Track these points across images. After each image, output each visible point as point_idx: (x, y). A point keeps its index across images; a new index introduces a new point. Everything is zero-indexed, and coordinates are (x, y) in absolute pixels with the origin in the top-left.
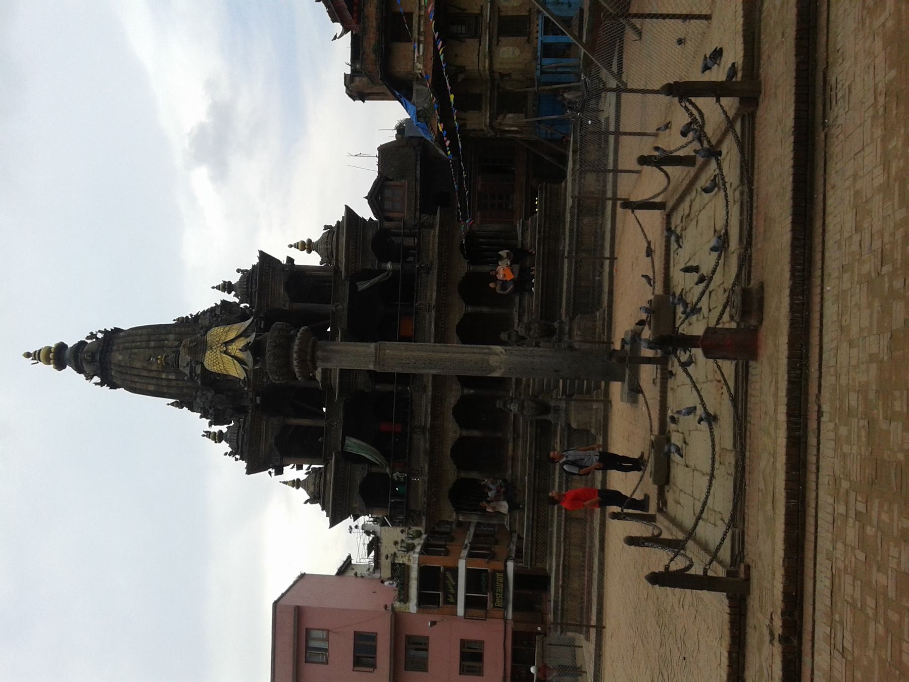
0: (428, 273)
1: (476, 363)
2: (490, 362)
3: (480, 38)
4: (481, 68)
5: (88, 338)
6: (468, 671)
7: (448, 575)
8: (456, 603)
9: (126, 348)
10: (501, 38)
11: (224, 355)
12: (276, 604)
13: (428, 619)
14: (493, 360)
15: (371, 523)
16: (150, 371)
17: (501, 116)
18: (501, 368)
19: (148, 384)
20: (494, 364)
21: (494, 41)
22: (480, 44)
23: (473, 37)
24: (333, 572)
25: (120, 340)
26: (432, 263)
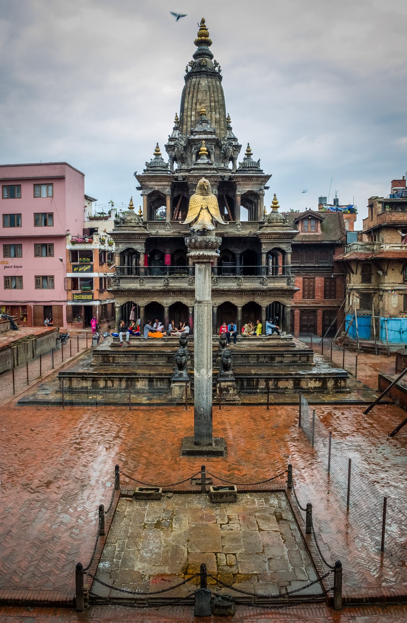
1: (202, 361)
3: (404, 284)
4: (385, 285)
5: (215, 61)
6: (37, 280)
7: (89, 267)
8: (73, 272)
9: (209, 88)
10: (403, 296)
12: (65, 164)
13: (64, 257)
14: (203, 371)
16: (196, 104)
17: (358, 295)
19: (188, 103)
20: (201, 372)
21: (401, 292)
22: (399, 284)
23: (404, 279)
24: (86, 193)
25: (214, 82)
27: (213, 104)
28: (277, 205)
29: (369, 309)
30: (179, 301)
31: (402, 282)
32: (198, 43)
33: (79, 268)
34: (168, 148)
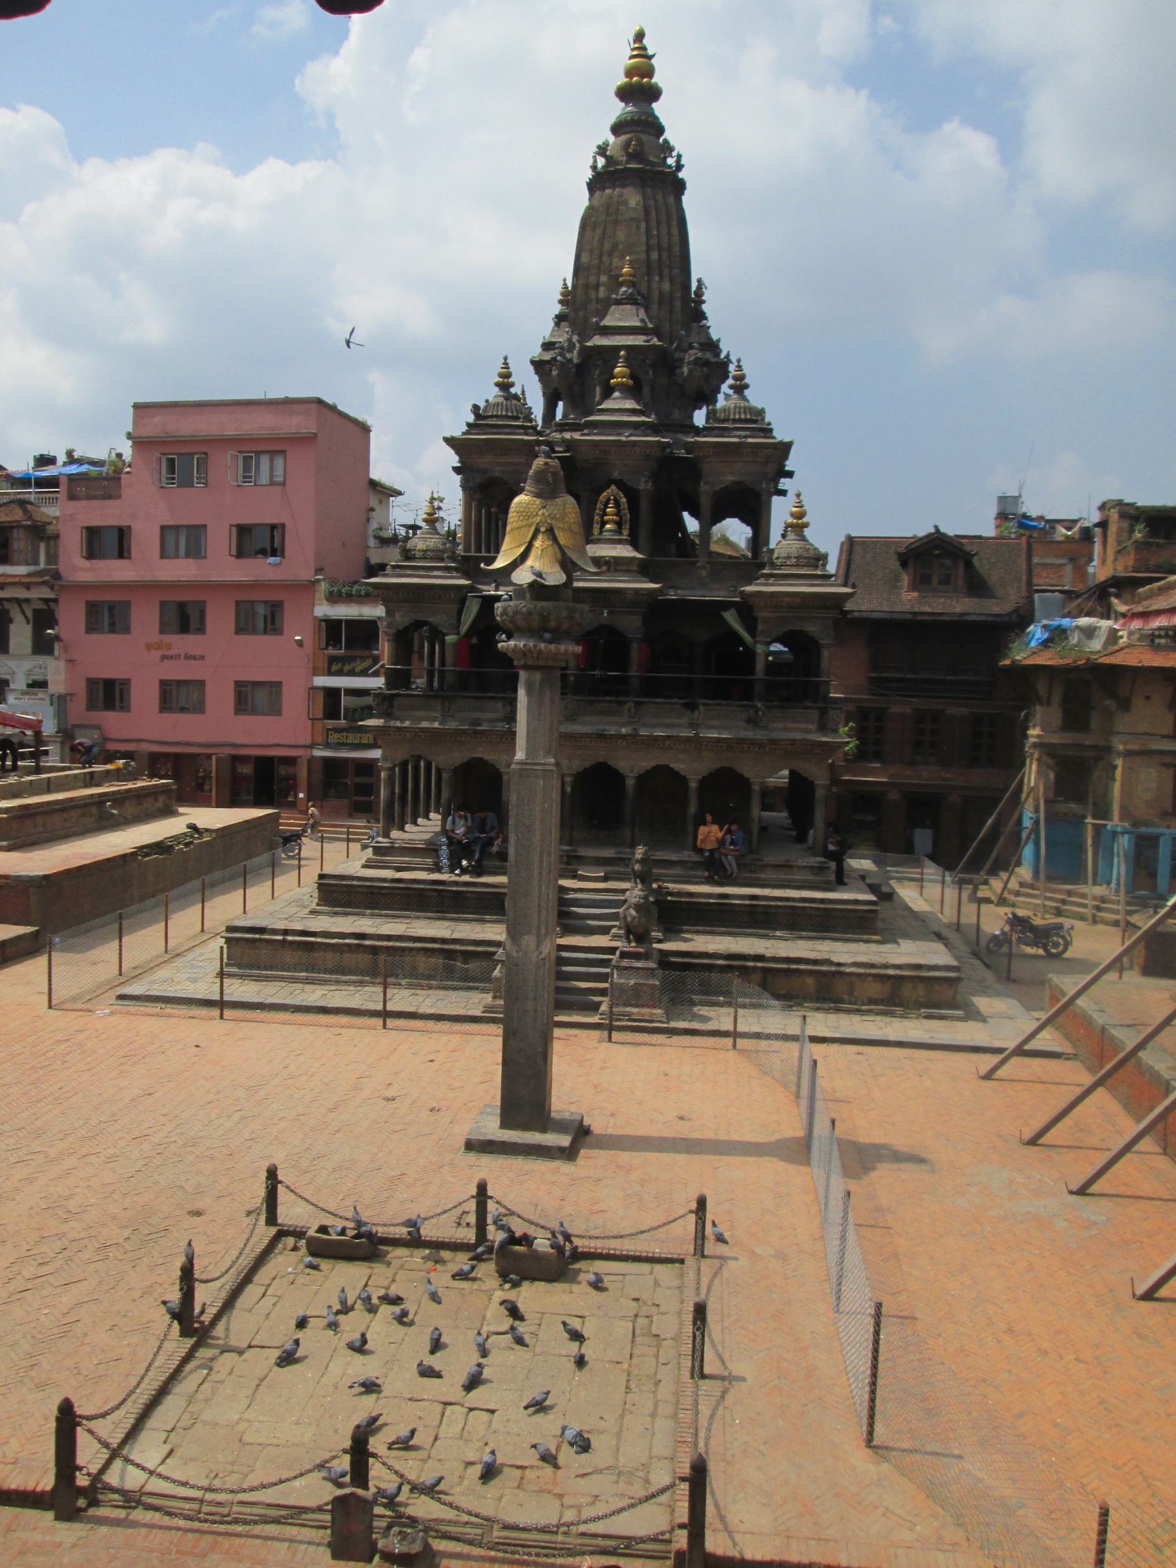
0: (749, 721)
8: (330, 673)
9: (647, 211)
11: (533, 529)
12: (319, 402)
15: (446, 529)
16: (610, 254)
18: (517, 951)
20: (524, 942)
21: (1168, 759)
24: (375, 475)
25: (660, 197)
26: (765, 728)
28: (805, 520)
31: (1171, 732)
32: (624, 94)
33: (344, 665)
34: (539, 366)
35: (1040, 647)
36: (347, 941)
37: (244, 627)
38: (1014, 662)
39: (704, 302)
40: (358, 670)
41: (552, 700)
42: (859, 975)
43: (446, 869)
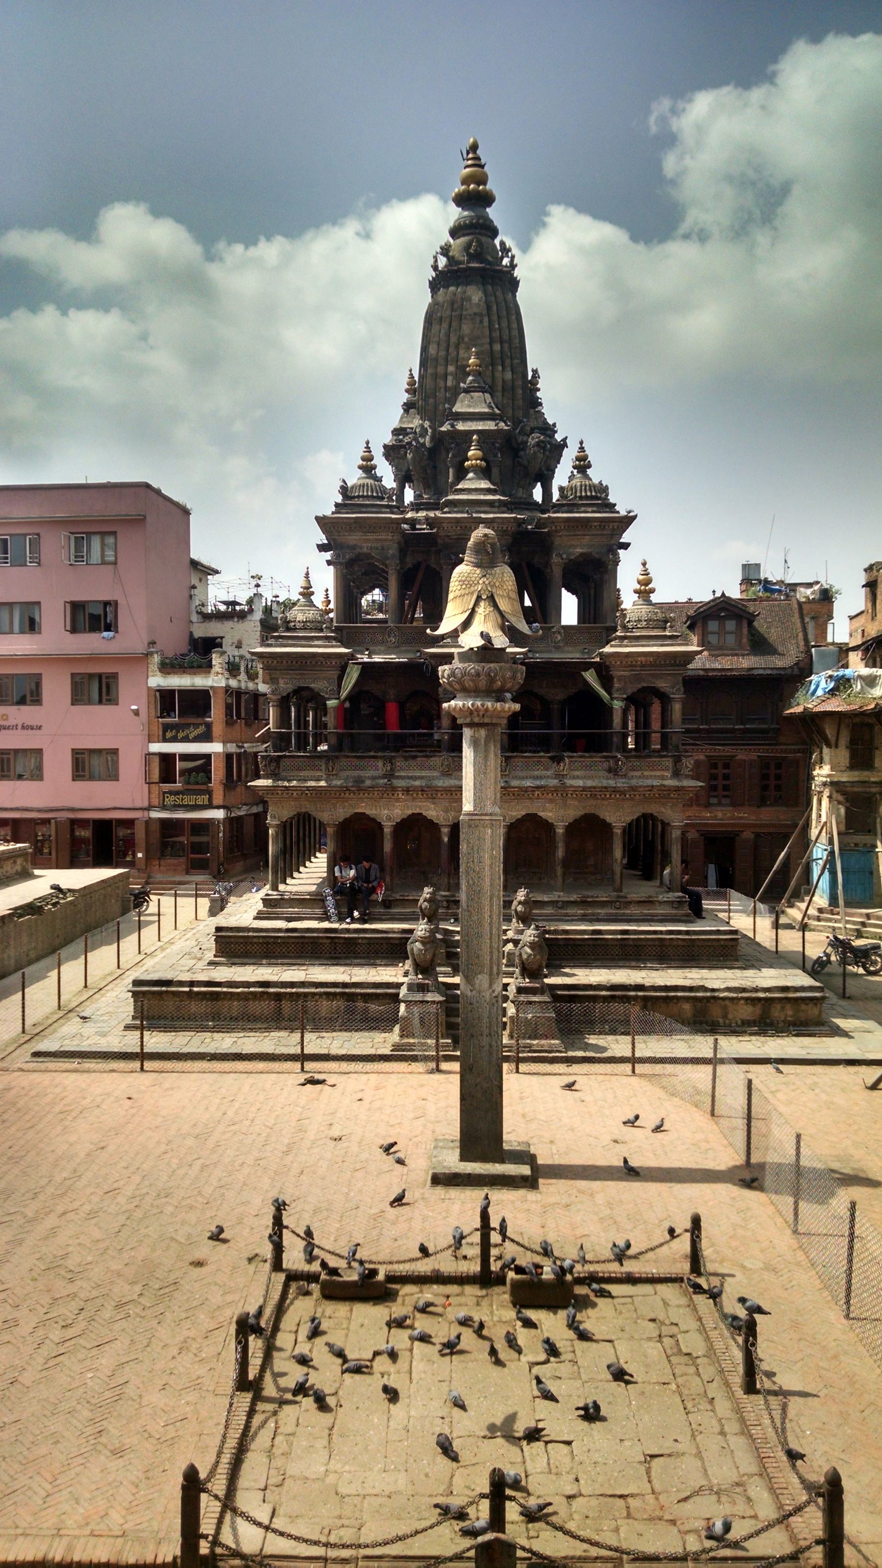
0: (610, 771)
1: (478, 957)
2: (479, 976)
5: (502, 243)
6: (77, 759)
7: (201, 729)
8: (165, 740)
9: (489, 308)
11: (475, 597)
12: (147, 486)
15: (264, 604)
16: (457, 347)
18: (471, 991)
19: (438, 344)
20: (477, 982)
24: (194, 555)
25: (499, 294)
27: (497, 347)
29: (869, 831)
30: (417, 811)
35: (827, 696)
36: (252, 989)
37: (79, 696)
38: (805, 709)
39: (539, 390)
40: (191, 736)
41: (496, 755)
42: (732, 999)
43: (334, 918)
